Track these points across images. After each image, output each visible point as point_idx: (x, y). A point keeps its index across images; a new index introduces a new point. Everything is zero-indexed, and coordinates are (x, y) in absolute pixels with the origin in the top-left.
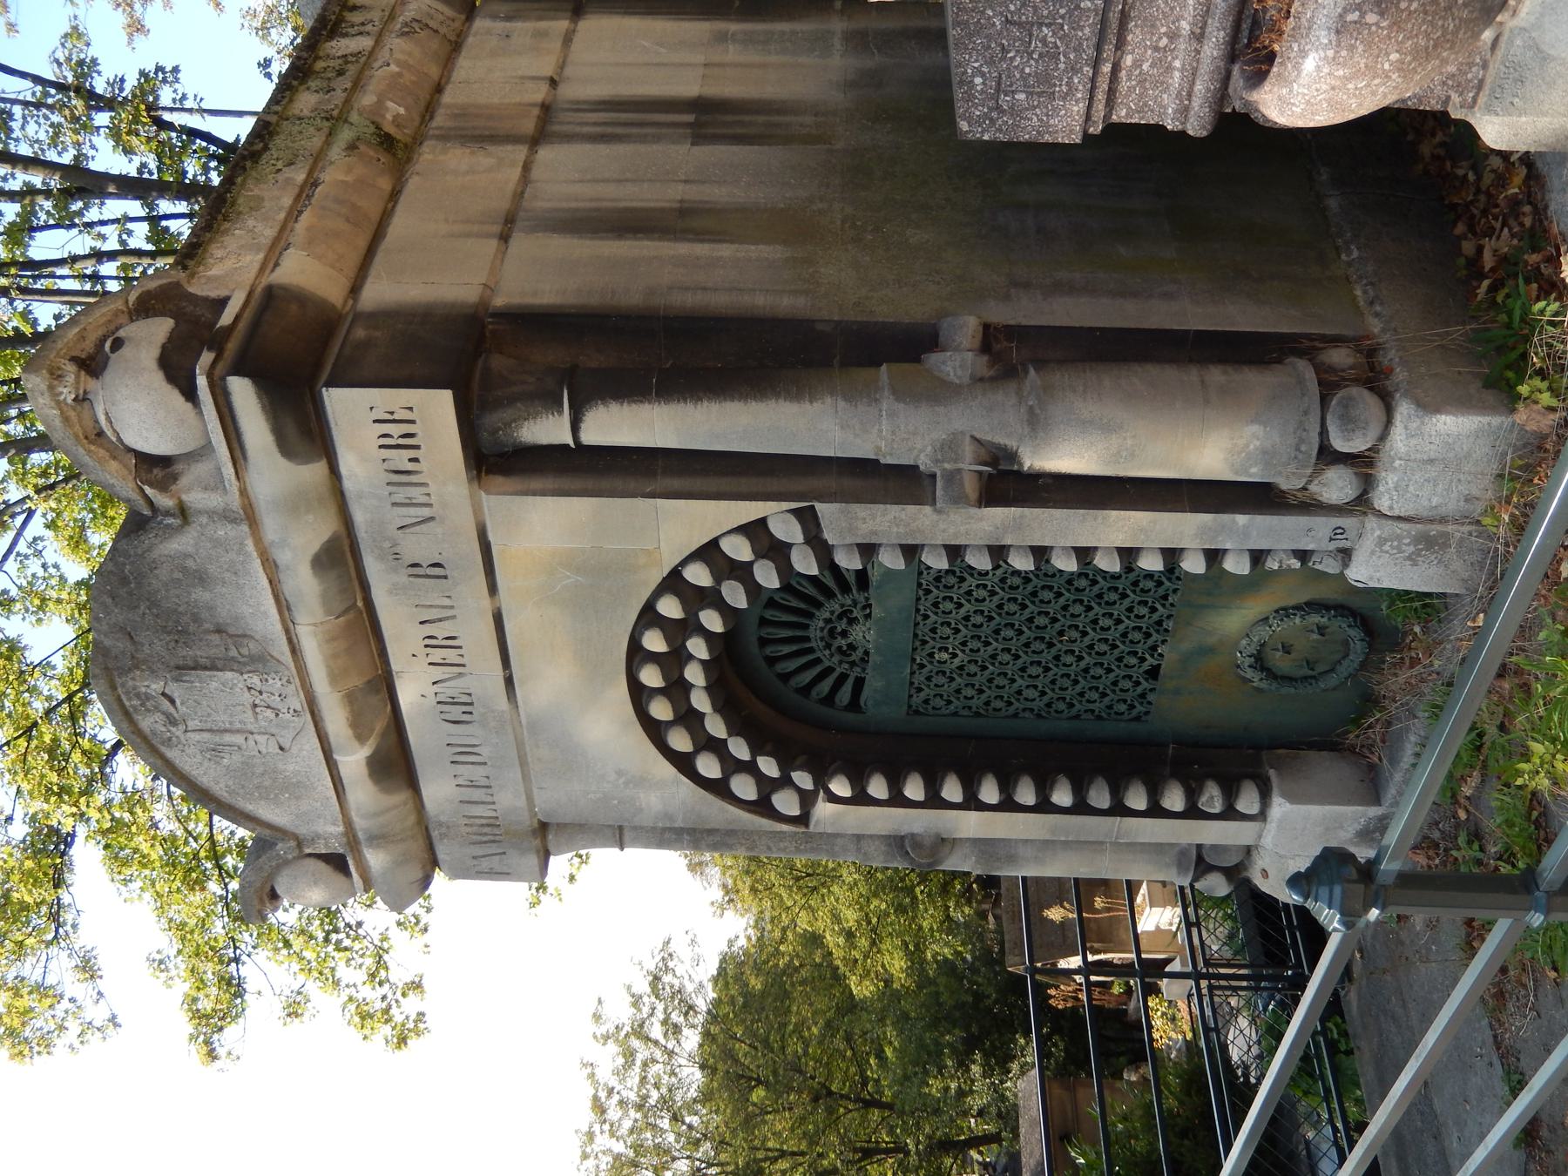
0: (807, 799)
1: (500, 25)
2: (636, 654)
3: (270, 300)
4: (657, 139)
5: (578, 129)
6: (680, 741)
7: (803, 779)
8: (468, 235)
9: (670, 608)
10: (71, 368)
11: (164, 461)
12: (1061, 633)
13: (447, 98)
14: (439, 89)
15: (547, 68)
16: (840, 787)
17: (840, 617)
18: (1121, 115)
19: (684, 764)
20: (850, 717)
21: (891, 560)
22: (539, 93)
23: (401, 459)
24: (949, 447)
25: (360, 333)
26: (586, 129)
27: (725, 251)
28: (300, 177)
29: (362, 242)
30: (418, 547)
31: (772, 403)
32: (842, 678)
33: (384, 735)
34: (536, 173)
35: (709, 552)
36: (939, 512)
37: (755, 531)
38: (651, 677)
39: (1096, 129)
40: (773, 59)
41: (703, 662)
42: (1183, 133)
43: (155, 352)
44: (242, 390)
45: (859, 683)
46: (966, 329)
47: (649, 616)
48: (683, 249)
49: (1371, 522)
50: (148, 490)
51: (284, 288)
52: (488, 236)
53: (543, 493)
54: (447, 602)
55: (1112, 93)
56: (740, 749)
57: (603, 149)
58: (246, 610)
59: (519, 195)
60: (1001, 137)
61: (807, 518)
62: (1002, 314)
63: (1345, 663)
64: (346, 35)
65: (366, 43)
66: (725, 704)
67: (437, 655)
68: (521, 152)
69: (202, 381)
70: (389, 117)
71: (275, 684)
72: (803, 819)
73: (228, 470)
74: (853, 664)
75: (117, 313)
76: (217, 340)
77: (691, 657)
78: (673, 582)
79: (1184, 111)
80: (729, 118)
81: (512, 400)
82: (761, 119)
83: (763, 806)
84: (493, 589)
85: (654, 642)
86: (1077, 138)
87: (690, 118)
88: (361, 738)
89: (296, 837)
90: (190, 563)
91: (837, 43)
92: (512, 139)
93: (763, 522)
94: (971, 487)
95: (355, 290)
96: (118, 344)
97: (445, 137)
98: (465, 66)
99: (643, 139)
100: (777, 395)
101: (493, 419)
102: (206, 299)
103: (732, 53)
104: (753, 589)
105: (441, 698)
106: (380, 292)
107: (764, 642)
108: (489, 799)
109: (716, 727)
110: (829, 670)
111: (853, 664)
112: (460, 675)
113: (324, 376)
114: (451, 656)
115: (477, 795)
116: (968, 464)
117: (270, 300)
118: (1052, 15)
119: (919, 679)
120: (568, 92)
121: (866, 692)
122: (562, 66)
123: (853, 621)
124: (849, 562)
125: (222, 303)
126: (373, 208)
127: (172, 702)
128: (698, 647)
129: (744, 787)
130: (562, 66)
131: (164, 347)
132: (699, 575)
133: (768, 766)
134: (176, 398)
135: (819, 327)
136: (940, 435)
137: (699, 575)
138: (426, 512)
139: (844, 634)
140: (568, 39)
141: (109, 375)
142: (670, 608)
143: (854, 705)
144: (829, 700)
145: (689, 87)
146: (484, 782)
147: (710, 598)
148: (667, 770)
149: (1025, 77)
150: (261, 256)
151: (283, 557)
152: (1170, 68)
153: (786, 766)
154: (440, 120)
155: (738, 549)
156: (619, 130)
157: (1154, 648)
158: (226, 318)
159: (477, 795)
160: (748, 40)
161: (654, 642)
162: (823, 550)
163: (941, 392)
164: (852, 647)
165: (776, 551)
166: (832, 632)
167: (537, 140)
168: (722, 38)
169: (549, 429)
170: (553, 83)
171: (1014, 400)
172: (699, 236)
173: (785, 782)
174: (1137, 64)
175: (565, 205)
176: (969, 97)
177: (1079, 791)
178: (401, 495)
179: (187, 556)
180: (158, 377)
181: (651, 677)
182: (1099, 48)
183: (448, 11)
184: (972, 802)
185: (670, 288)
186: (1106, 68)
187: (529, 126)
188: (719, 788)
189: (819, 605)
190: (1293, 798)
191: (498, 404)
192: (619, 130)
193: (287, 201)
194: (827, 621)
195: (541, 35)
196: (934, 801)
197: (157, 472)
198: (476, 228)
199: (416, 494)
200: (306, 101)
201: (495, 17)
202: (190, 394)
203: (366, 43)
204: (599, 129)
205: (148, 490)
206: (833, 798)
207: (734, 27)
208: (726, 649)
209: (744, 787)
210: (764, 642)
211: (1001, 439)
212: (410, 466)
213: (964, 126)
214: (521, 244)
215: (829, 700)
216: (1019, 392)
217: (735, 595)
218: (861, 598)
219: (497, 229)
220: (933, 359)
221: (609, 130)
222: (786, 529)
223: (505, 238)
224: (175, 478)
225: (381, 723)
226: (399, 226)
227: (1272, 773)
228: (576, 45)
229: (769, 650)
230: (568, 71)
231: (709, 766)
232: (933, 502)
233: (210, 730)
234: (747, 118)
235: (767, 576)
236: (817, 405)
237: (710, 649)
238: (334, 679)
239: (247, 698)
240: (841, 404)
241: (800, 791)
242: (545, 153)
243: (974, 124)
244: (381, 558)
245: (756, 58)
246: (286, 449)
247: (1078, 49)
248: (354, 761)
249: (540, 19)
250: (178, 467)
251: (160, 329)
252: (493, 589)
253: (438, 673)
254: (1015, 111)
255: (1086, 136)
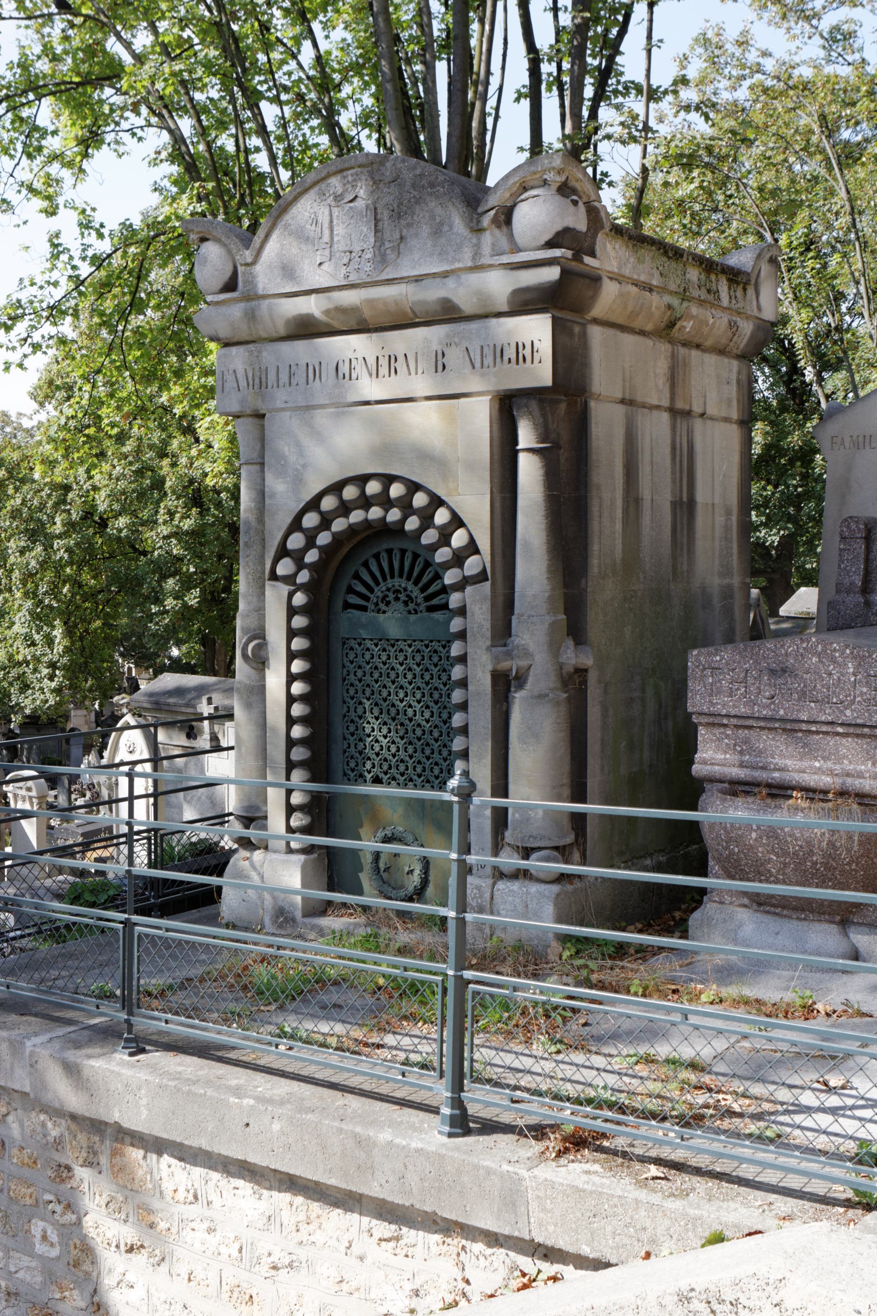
0: (289, 579)
1: (734, 376)
2: (388, 480)
3: (595, 280)
4: (674, 481)
5: (678, 434)
6: (328, 503)
7: (304, 577)
8: (624, 381)
9: (420, 500)
10: (563, 179)
11: (508, 221)
12: (402, 724)
13: (695, 353)
14: (698, 346)
15: (711, 411)
16: (299, 599)
17: (408, 596)
18: (702, 731)
19: (314, 504)
20: (340, 604)
21: (456, 625)
22: (697, 409)
23: (510, 353)
24: (527, 654)
25: (577, 329)
26: (678, 439)
27: (619, 526)
28: (655, 282)
29: (620, 321)
30: (455, 356)
31: (546, 557)
32: (367, 599)
33: (327, 325)
34: (655, 413)
35: (457, 522)
36: (488, 649)
37: (472, 548)
38: (373, 487)
39: (695, 719)
40: (717, 543)
41: (385, 518)
42: (692, 762)
43: (571, 226)
44: (552, 274)
45: (364, 609)
46: (587, 660)
47: (414, 487)
48: (619, 503)
49: (490, 881)
50: (493, 212)
51: (600, 287)
52: (624, 392)
53: (491, 431)
54: (420, 371)
55: (713, 725)
56: (324, 539)
57: (667, 450)
58: (417, 255)
59: (644, 406)
60: (690, 671)
61: (482, 577)
62: (592, 678)
63: (390, 889)
64: (730, 289)
65: (725, 302)
66: (352, 530)
67: (384, 362)
68: (666, 403)
69: (557, 253)
70: (685, 324)
71: (368, 267)
72: (274, 577)
73: (505, 259)
74: (377, 604)
75: (589, 196)
76: (577, 257)
77: (387, 511)
78: (437, 502)
79: (704, 762)
80: (685, 522)
81: (544, 416)
82: (685, 540)
83: (283, 552)
84: (429, 398)
85: (396, 490)
86: (690, 709)
87: (685, 499)
88: (327, 312)
89: (254, 262)
90: (446, 228)
91: (726, 581)
92: (673, 398)
93: (477, 551)
94: (504, 665)
95: (596, 321)
96: (575, 203)
97: (673, 356)
98: (711, 359)
99: (673, 473)
100: (550, 560)
101: (534, 405)
102: (595, 243)
103: (720, 520)
104: (433, 548)
105: (354, 362)
106: (596, 334)
107: (390, 552)
108: (281, 384)
109: (339, 525)
110: (371, 591)
111: (377, 604)
112: (371, 375)
113: (559, 314)
114: (384, 370)
115: (284, 378)
116: (513, 665)
117: (595, 280)
118: (751, 693)
119: (369, 644)
120: (698, 424)
121: (357, 613)
122: (712, 419)
123: (406, 603)
124: (455, 600)
125: (593, 254)
126: (637, 324)
127: (351, 201)
128: (394, 515)
129: (296, 541)
130: (712, 419)
131: (574, 229)
132: (441, 517)
133: (312, 557)
134: (547, 237)
135: (583, 581)
136: (532, 647)
137: (441, 517)
138: (478, 364)
139: (397, 599)
140: (727, 420)
141: (558, 198)
142: (420, 500)
143: (347, 606)
144: (351, 590)
145: (701, 497)
146: (294, 382)
147: (427, 520)
148: (308, 495)
149: (720, 681)
150: (616, 270)
151: (450, 282)
152: (726, 753)
153: (312, 567)
154: (682, 351)
155: (459, 539)
156: (678, 458)
157: (394, 779)
158: (587, 260)
159: (284, 378)
160: (727, 528)
161: (396, 490)
162: (460, 586)
163: (554, 648)
164: (388, 603)
165: (458, 559)
166: (397, 591)
167: (673, 411)
168: (728, 513)
169: (526, 436)
170: (702, 415)
171: (551, 685)
172: (626, 511)
173: (300, 565)
174: (727, 736)
175: (639, 433)
176: (710, 654)
177: (302, 742)
178: (488, 352)
179: (451, 227)
180: (558, 227)
181: (373, 487)
182: (735, 716)
183: (742, 346)
184: (291, 678)
185: (600, 498)
186: (725, 721)
187: (680, 405)
188: (296, 525)
189: (416, 583)
190: (304, 868)
191: (542, 409)
192: (678, 458)
193: (643, 278)
194: (405, 590)
195: (729, 405)
196: (291, 656)
197: (502, 218)
198: (628, 384)
199: (489, 360)
200: (694, 274)
201: (739, 373)
202: (550, 244)
203: (725, 302)
204: (678, 446)
205: (493, 212)
206: (291, 595)
207: (734, 518)
208: (397, 530)
209: (296, 541)
210: (390, 552)
211: (531, 680)
212: (506, 358)
213: (695, 652)
214: (621, 409)
215: (351, 590)
216: (555, 689)
217: (429, 537)
218: (423, 607)
219: (627, 397)
220: (570, 643)
221: (678, 452)
222: (472, 565)
223: (623, 401)
224: (499, 227)
225: (337, 325)
226: (629, 339)
227: (315, 855)
228: (724, 426)
229: (384, 557)
230: (709, 422)
231: (310, 520)
232: (493, 646)
233: (331, 221)
234: (685, 532)
235: (442, 555)
236: (545, 581)
237: (394, 523)
238: (370, 302)
239: (357, 248)
240: (547, 595)
241: (295, 575)
242: (665, 417)
243: (696, 657)
244: (448, 336)
245: (717, 534)
246: (517, 292)
247: (734, 706)
248: (312, 306)
249: (738, 401)
250: (505, 229)
251: (581, 224)
252: (429, 398)
253: (371, 361)
254: (703, 676)
255: (691, 714)
